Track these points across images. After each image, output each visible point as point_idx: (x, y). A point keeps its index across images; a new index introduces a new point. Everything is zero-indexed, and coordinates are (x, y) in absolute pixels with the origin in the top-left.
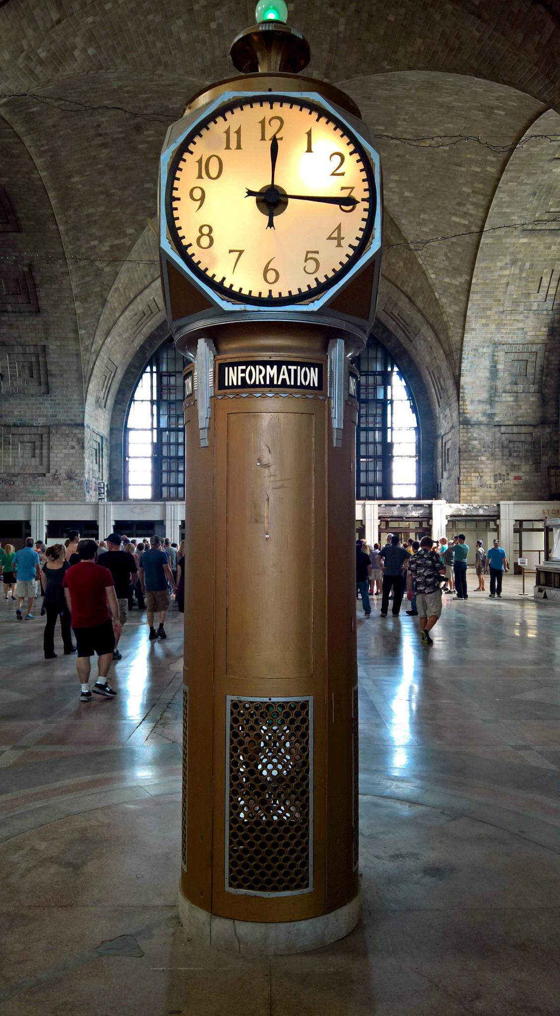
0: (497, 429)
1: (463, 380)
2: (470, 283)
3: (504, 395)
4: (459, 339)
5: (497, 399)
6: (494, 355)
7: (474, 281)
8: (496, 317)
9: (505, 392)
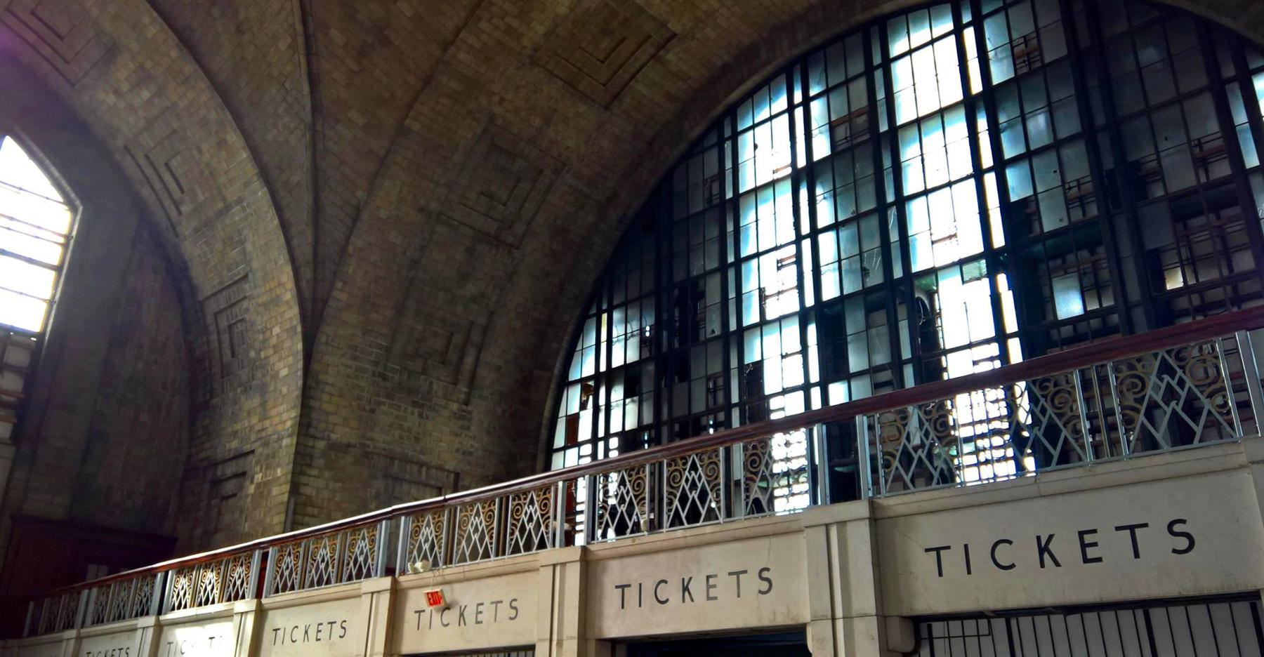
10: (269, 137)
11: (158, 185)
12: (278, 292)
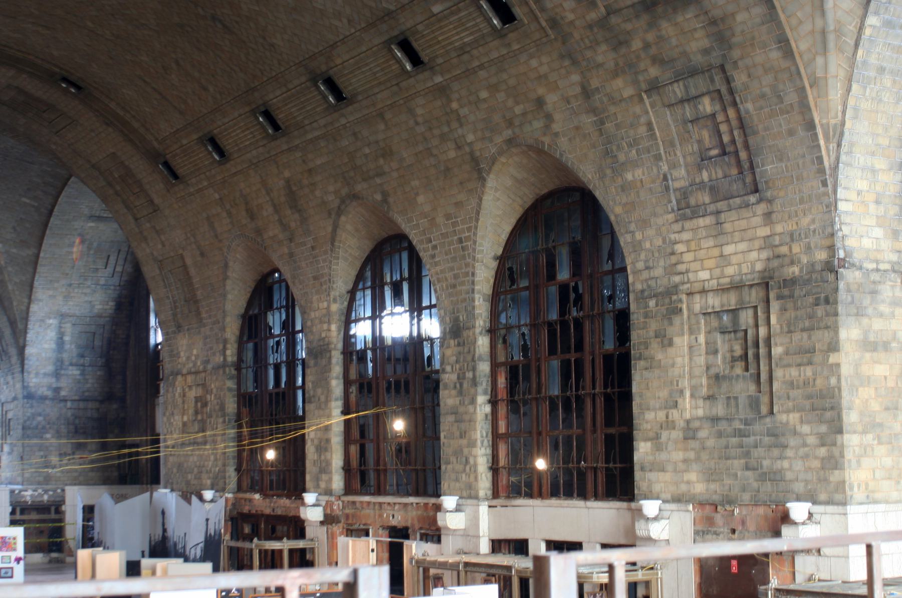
0: (62, 404)
1: (29, 351)
2: (37, 256)
3: (70, 368)
4: (24, 308)
5: (63, 372)
6: (60, 327)
7: (42, 255)
8: (64, 290)
9: (71, 364)
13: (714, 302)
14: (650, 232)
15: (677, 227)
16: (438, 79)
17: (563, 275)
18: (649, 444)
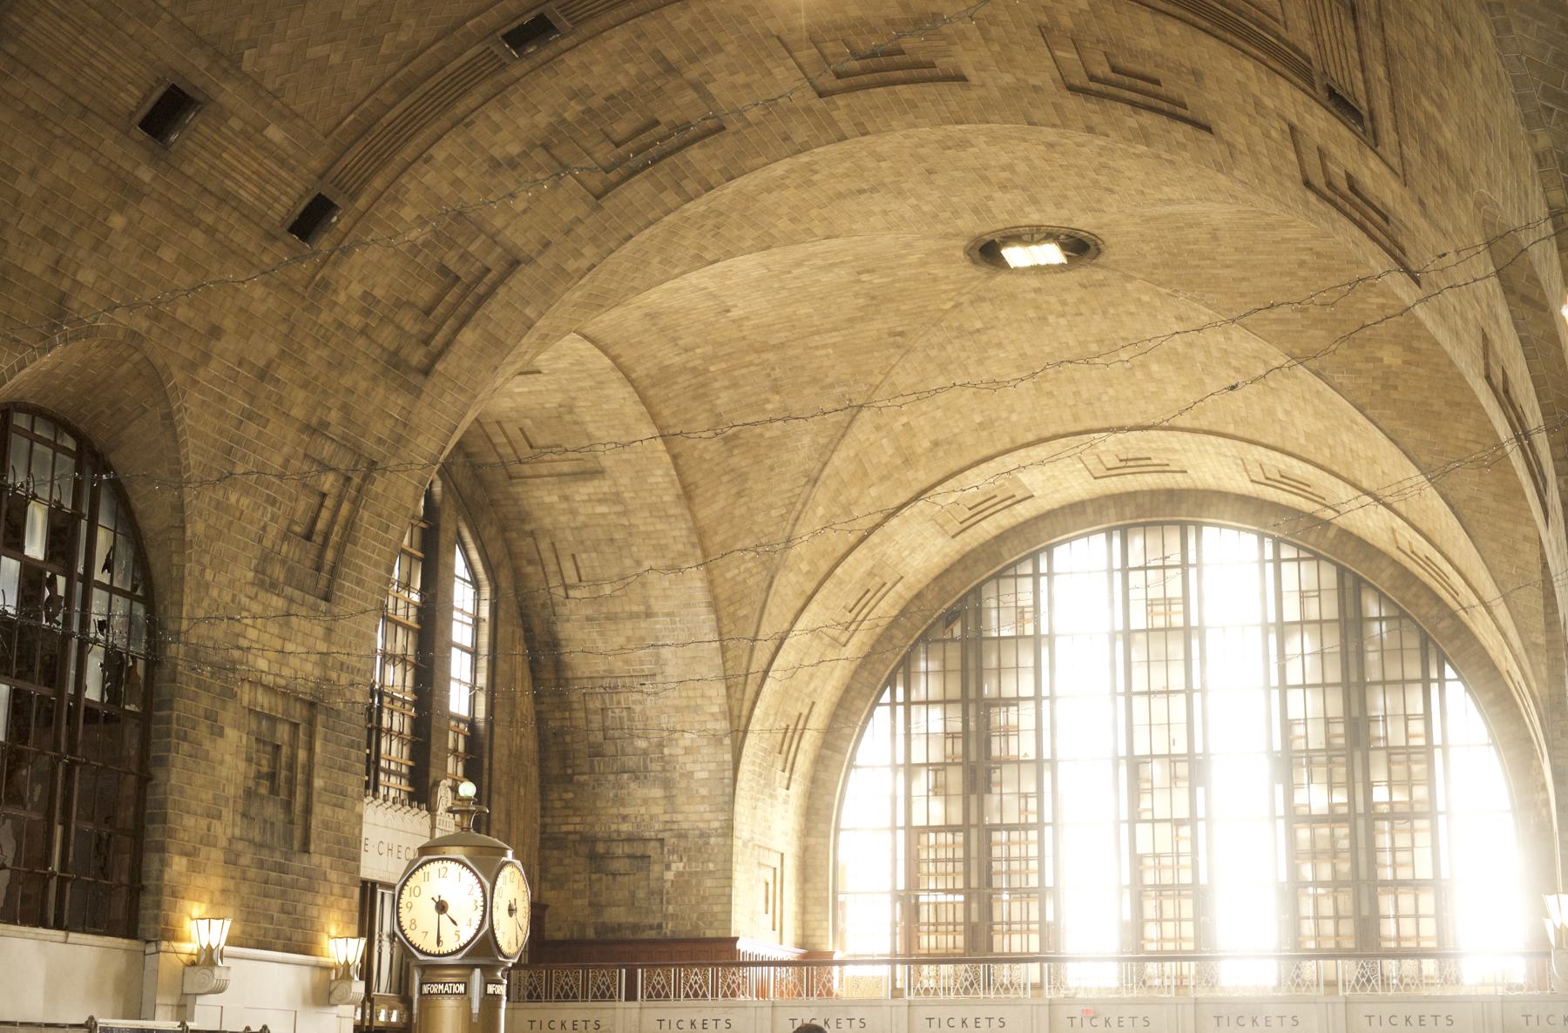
10: (729, 575)
11: (552, 568)
12: (699, 701)
13: (263, 700)
14: (223, 578)
15: (252, 591)
16: (145, 174)
17: (35, 548)
18: (184, 860)
